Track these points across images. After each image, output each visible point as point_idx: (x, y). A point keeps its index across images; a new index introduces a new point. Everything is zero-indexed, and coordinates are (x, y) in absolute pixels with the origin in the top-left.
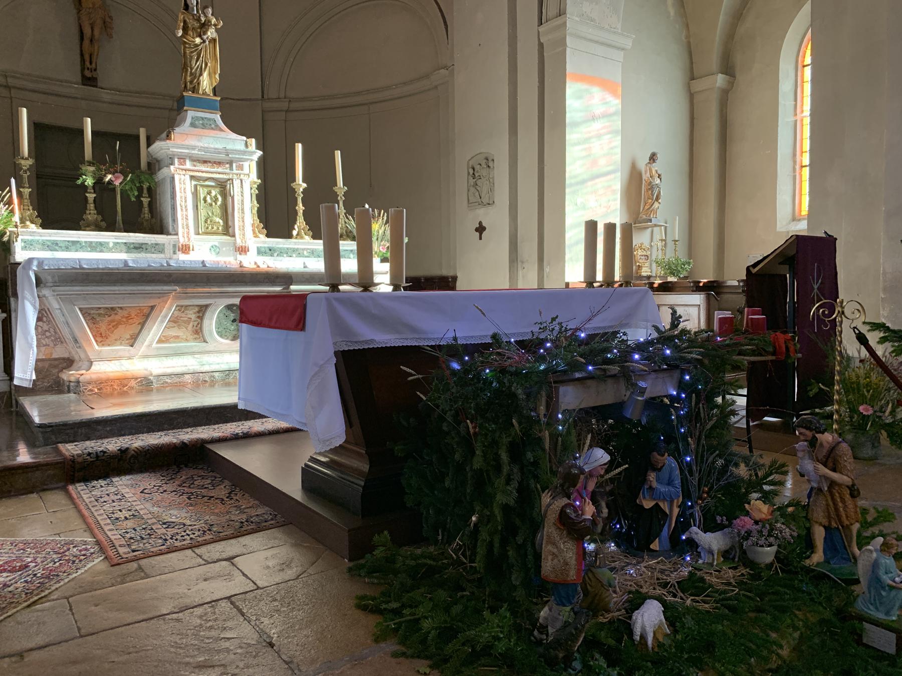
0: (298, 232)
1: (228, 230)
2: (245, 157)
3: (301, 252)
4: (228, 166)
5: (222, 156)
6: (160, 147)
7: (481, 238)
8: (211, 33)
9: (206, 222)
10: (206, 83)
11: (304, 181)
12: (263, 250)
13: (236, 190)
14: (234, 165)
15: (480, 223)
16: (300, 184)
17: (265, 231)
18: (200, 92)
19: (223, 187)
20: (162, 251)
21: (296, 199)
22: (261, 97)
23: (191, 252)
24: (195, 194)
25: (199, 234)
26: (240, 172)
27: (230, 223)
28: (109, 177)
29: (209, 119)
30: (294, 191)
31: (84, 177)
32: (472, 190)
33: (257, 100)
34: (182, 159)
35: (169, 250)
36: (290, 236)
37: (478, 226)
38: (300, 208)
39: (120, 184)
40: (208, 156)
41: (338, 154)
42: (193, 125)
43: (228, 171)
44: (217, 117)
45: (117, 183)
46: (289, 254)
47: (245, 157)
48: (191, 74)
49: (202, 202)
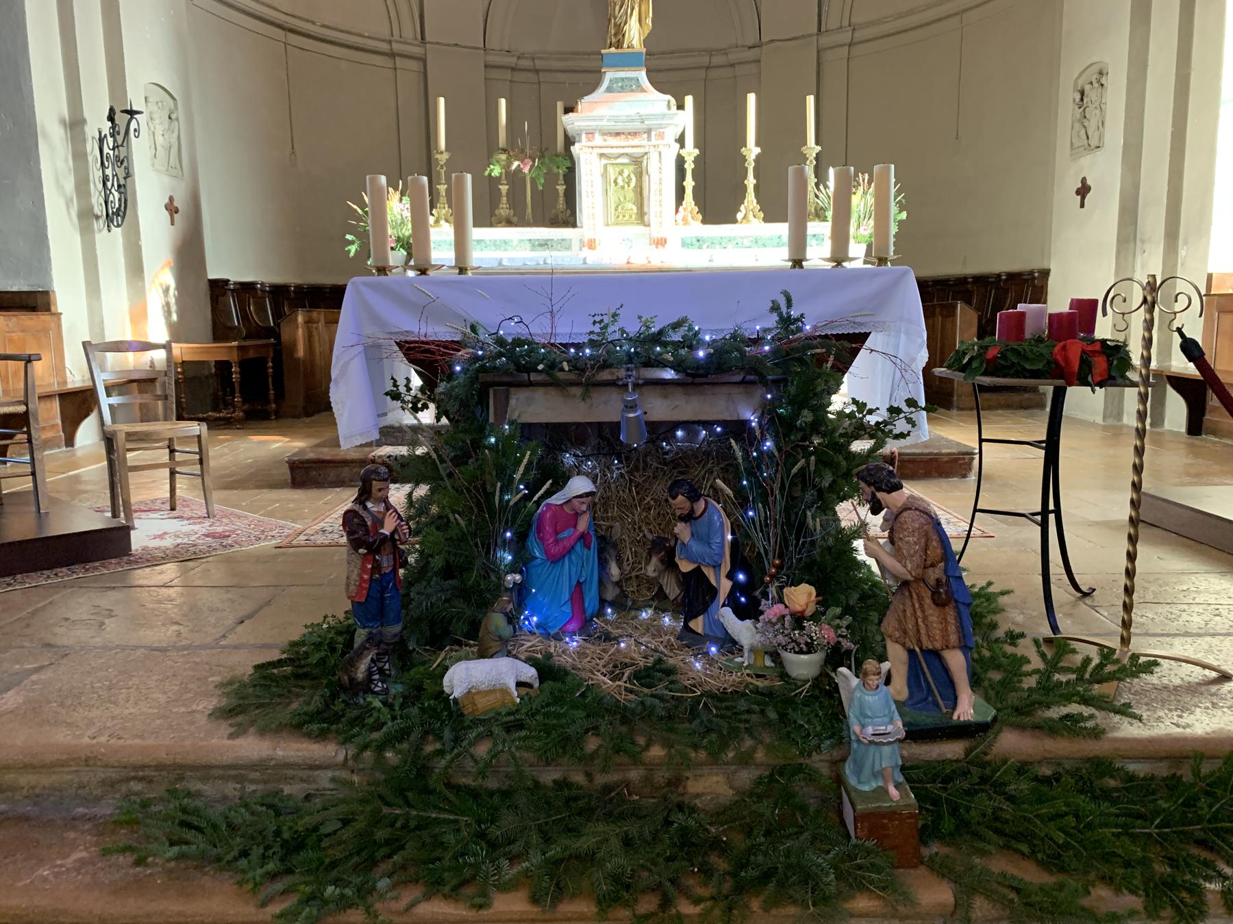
0: (745, 215)
1: (641, 216)
2: (664, 122)
3: (739, 241)
4: (645, 136)
5: (636, 126)
6: (570, 122)
7: (1082, 206)
9: (617, 207)
10: (635, 33)
11: (758, 144)
12: (689, 241)
13: (652, 165)
14: (653, 133)
15: (1084, 180)
16: (752, 150)
17: (700, 217)
18: (625, 45)
19: (638, 162)
20: (568, 248)
21: (746, 169)
22: (815, 30)
23: (598, 248)
24: (605, 174)
25: (608, 225)
26: (660, 142)
27: (646, 209)
28: (516, 164)
29: (630, 79)
30: (744, 159)
31: (492, 167)
32: (1077, 126)
33: (810, 36)
35: (576, 245)
36: (735, 221)
37: (1080, 185)
38: (751, 181)
39: (530, 170)
40: (620, 127)
42: (609, 90)
43: (642, 143)
44: (642, 75)
45: (526, 170)
46: (724, 245)
47: (664, 122)
48: (615, 24)
49: (613, 184)
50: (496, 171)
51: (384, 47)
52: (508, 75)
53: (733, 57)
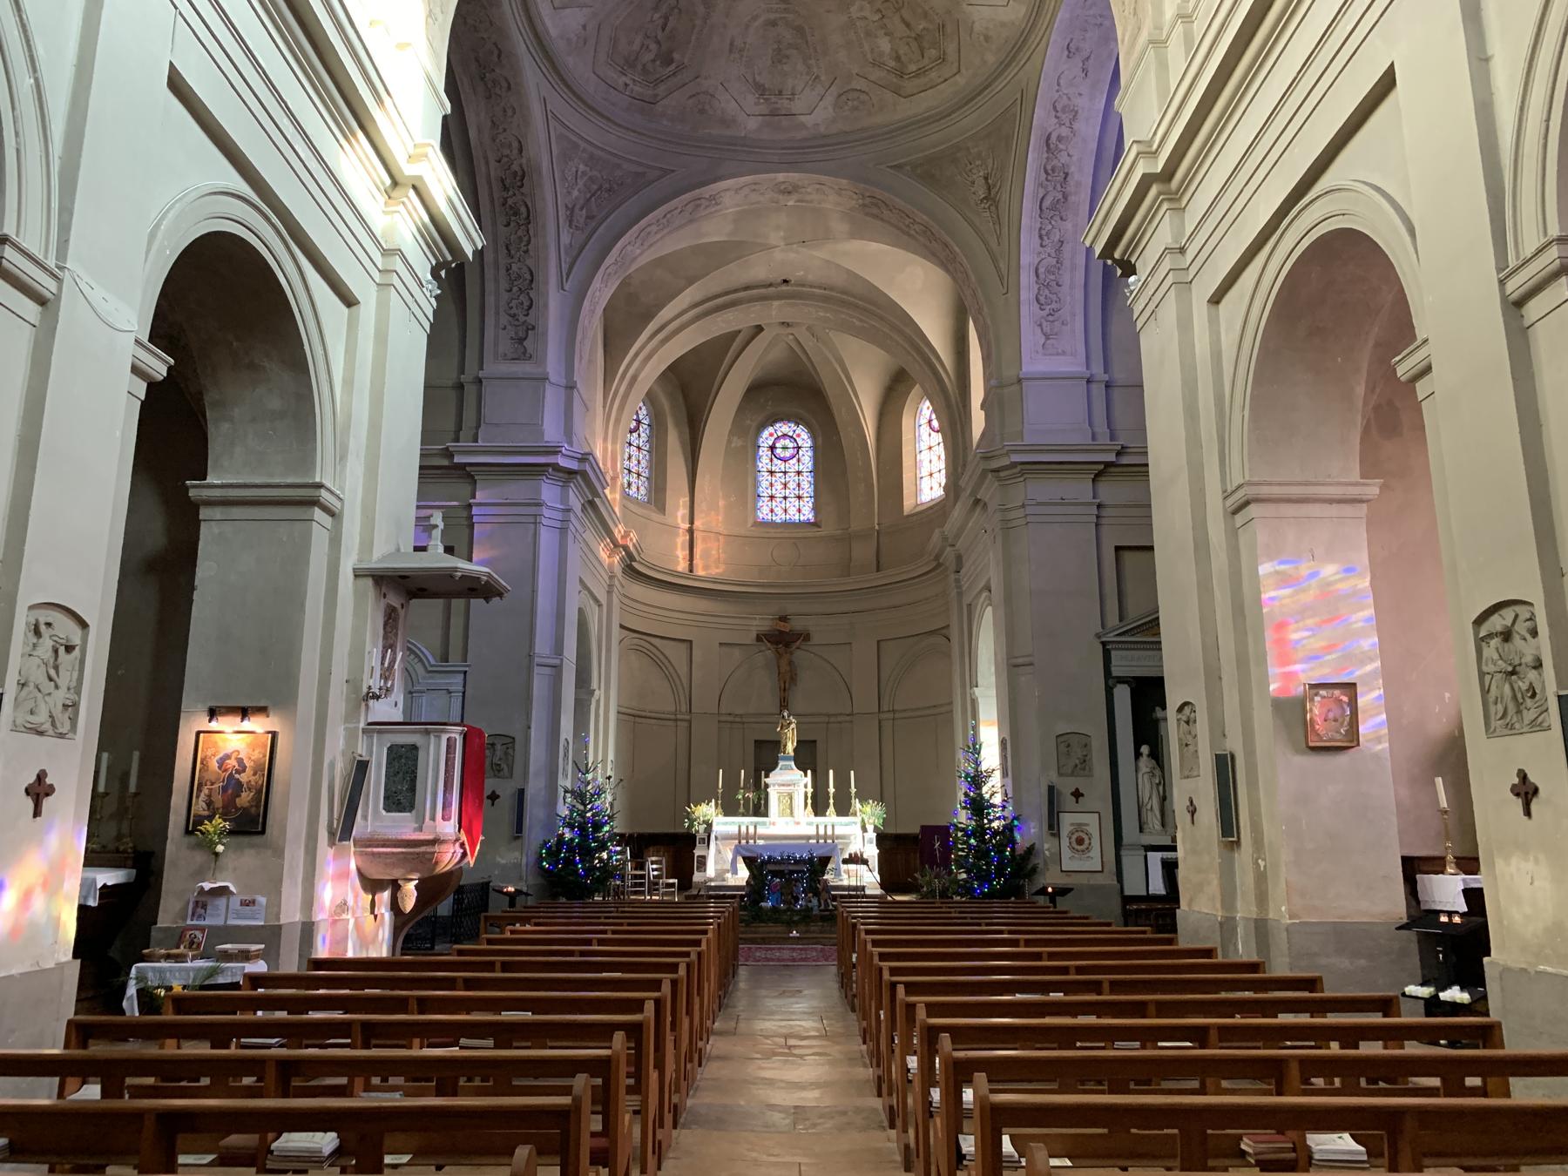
1: (792, 814)
8: (793, 726)
13: (795, 797)
16: (832, 790)
30: (828, 793)
34: (774, 785)
38: (831, 801)
41: (852, 772)
44: (793, 763)
50: (740, 797)
51: (673, 717)
52: (729, 725)
53: (840, 719)
